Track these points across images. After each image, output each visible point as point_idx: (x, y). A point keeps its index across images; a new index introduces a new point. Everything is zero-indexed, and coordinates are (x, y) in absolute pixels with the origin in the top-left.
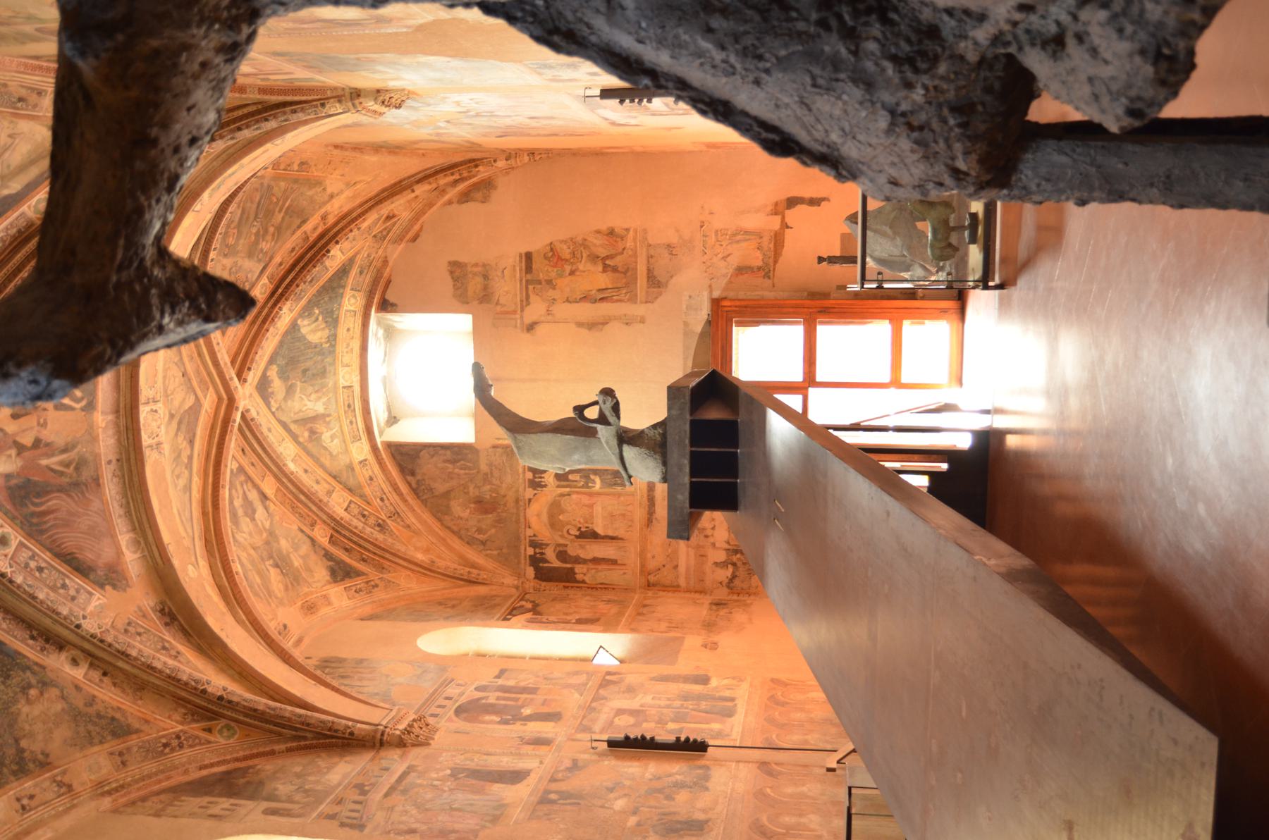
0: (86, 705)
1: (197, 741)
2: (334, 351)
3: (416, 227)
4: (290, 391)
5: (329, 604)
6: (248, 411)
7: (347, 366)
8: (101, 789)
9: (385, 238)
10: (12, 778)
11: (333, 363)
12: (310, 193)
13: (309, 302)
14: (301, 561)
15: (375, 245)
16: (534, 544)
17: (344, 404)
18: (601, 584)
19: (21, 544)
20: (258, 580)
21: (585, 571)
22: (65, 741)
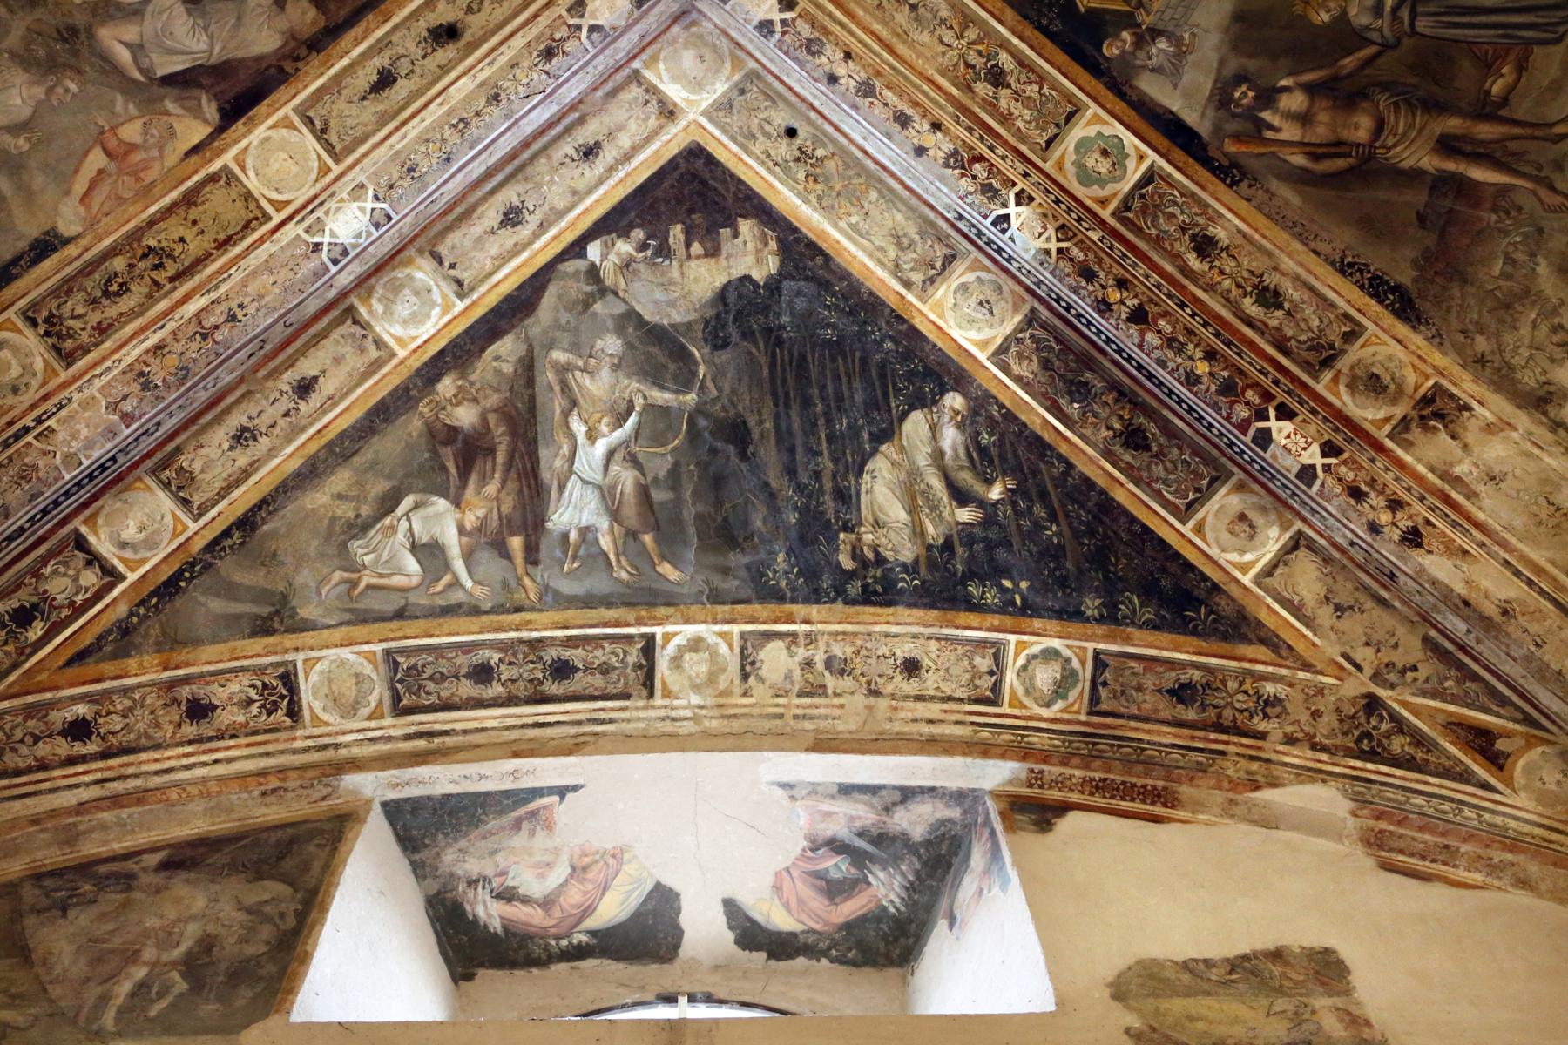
2: (815, 597)
7: (747, 668)
9: (1371, 755)
13: (1040, 446)
15: (1328, 721)
17: (571, 642)
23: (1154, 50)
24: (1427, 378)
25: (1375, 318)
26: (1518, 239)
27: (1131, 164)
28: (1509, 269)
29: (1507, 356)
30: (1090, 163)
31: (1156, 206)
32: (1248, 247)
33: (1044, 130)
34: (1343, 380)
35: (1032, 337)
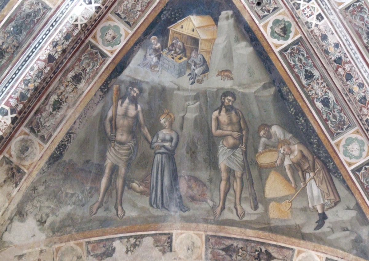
12: (67, 209)
23: (153, 56)
24: (28, 169)
25: (50, 147)
26: (80, 198)
27: (110, 48)
28: (69, 195)
29: (37, 198)
30: (110, 32)
31: (93, 59)
32: (77, 96)
33: (123, 13)
34: (26, 137)
35: (40, 9)
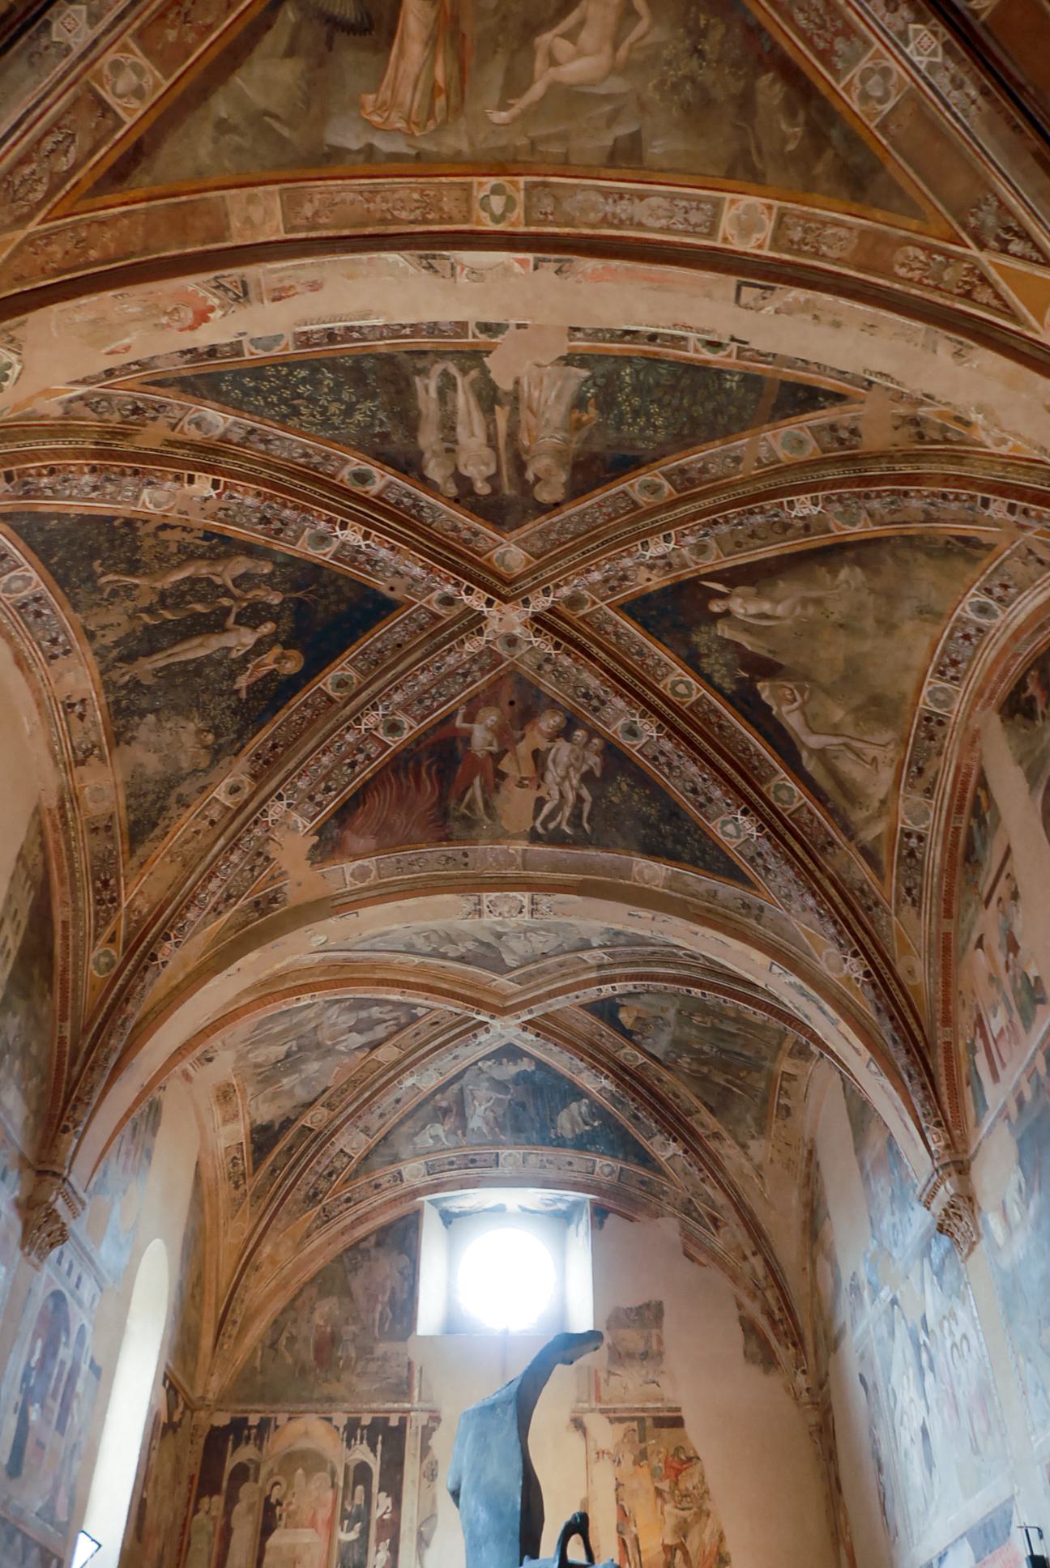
0: (180, 795)
1: (102, 923)
2: (544, 1144)
3: (703, 1259)
4: (500, 1085)
5: (225, 1122)
6: (487, 1031)
8: (69, 798)
10: (112, 698)
11: (529, 1142)
12: (749, 1118)
13: (610, 1115)
14: (287, 1087)
15: (678, 1203)
16: (264, 1426)
18: (189, 1543)
19: (387, 747)
20: (277, 1029)
21: (214, 1513)
22: (141, 765)
25: (704, 1110)
